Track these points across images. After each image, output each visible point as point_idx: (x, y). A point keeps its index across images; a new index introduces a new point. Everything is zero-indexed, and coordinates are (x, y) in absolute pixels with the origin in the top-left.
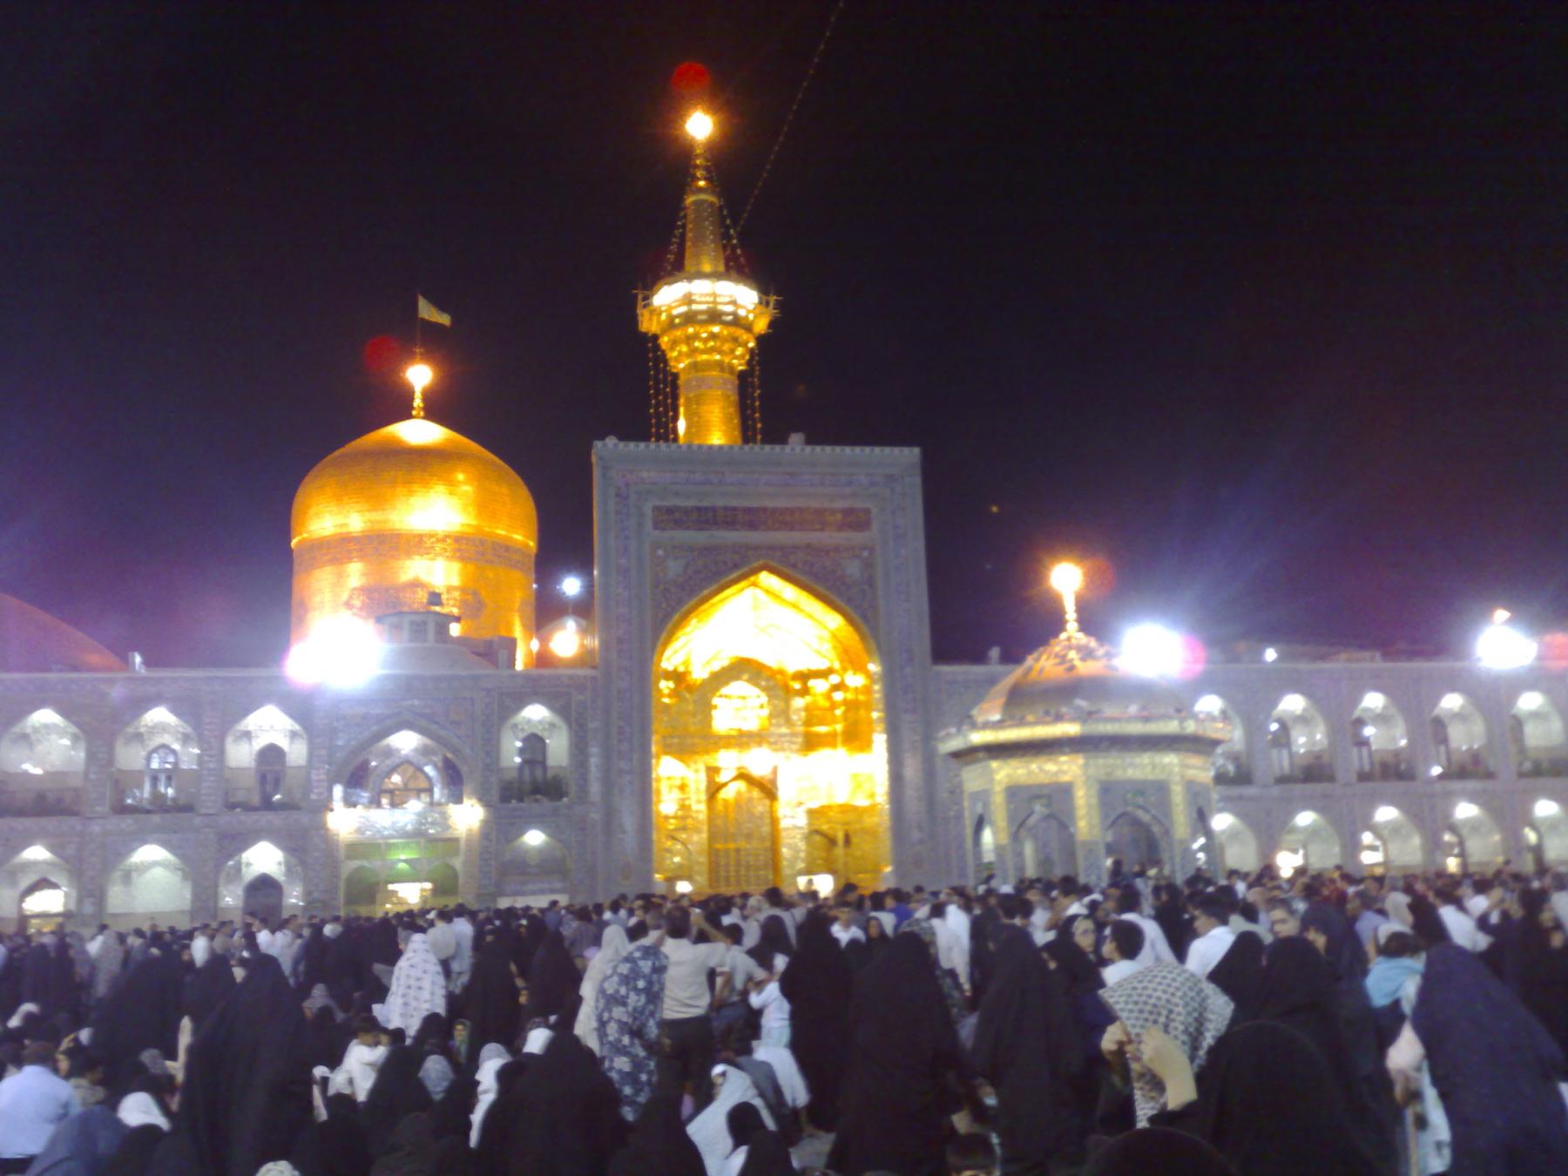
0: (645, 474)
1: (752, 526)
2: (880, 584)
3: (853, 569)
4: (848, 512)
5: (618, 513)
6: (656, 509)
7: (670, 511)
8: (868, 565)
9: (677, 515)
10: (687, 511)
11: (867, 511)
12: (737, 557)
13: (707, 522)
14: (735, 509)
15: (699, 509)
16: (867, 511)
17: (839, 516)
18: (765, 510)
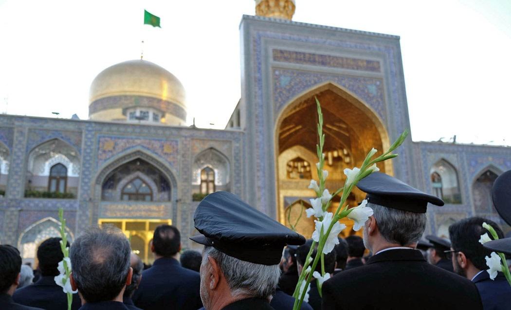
0: (268, 33)
1: (323, 63)
2: (386, 98)
3: (372, 89)
4: (368, 62)
5: (255, 50)
6: (274, 50)
7: (282, 52)
8: (380, 88)
9: (285, 55)
10: (290, 53)
11: (378, 63)
12: (316, 79)
13: (301, 60)
14: (314, 55)
15: (296, 53)
16: (378, 63)
17: (365, 63)
18: (329, 56)
